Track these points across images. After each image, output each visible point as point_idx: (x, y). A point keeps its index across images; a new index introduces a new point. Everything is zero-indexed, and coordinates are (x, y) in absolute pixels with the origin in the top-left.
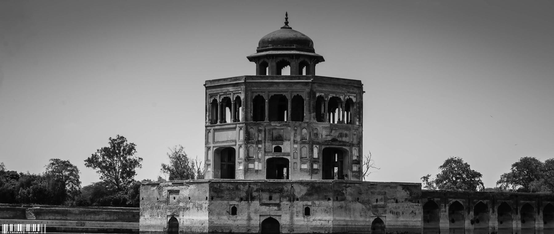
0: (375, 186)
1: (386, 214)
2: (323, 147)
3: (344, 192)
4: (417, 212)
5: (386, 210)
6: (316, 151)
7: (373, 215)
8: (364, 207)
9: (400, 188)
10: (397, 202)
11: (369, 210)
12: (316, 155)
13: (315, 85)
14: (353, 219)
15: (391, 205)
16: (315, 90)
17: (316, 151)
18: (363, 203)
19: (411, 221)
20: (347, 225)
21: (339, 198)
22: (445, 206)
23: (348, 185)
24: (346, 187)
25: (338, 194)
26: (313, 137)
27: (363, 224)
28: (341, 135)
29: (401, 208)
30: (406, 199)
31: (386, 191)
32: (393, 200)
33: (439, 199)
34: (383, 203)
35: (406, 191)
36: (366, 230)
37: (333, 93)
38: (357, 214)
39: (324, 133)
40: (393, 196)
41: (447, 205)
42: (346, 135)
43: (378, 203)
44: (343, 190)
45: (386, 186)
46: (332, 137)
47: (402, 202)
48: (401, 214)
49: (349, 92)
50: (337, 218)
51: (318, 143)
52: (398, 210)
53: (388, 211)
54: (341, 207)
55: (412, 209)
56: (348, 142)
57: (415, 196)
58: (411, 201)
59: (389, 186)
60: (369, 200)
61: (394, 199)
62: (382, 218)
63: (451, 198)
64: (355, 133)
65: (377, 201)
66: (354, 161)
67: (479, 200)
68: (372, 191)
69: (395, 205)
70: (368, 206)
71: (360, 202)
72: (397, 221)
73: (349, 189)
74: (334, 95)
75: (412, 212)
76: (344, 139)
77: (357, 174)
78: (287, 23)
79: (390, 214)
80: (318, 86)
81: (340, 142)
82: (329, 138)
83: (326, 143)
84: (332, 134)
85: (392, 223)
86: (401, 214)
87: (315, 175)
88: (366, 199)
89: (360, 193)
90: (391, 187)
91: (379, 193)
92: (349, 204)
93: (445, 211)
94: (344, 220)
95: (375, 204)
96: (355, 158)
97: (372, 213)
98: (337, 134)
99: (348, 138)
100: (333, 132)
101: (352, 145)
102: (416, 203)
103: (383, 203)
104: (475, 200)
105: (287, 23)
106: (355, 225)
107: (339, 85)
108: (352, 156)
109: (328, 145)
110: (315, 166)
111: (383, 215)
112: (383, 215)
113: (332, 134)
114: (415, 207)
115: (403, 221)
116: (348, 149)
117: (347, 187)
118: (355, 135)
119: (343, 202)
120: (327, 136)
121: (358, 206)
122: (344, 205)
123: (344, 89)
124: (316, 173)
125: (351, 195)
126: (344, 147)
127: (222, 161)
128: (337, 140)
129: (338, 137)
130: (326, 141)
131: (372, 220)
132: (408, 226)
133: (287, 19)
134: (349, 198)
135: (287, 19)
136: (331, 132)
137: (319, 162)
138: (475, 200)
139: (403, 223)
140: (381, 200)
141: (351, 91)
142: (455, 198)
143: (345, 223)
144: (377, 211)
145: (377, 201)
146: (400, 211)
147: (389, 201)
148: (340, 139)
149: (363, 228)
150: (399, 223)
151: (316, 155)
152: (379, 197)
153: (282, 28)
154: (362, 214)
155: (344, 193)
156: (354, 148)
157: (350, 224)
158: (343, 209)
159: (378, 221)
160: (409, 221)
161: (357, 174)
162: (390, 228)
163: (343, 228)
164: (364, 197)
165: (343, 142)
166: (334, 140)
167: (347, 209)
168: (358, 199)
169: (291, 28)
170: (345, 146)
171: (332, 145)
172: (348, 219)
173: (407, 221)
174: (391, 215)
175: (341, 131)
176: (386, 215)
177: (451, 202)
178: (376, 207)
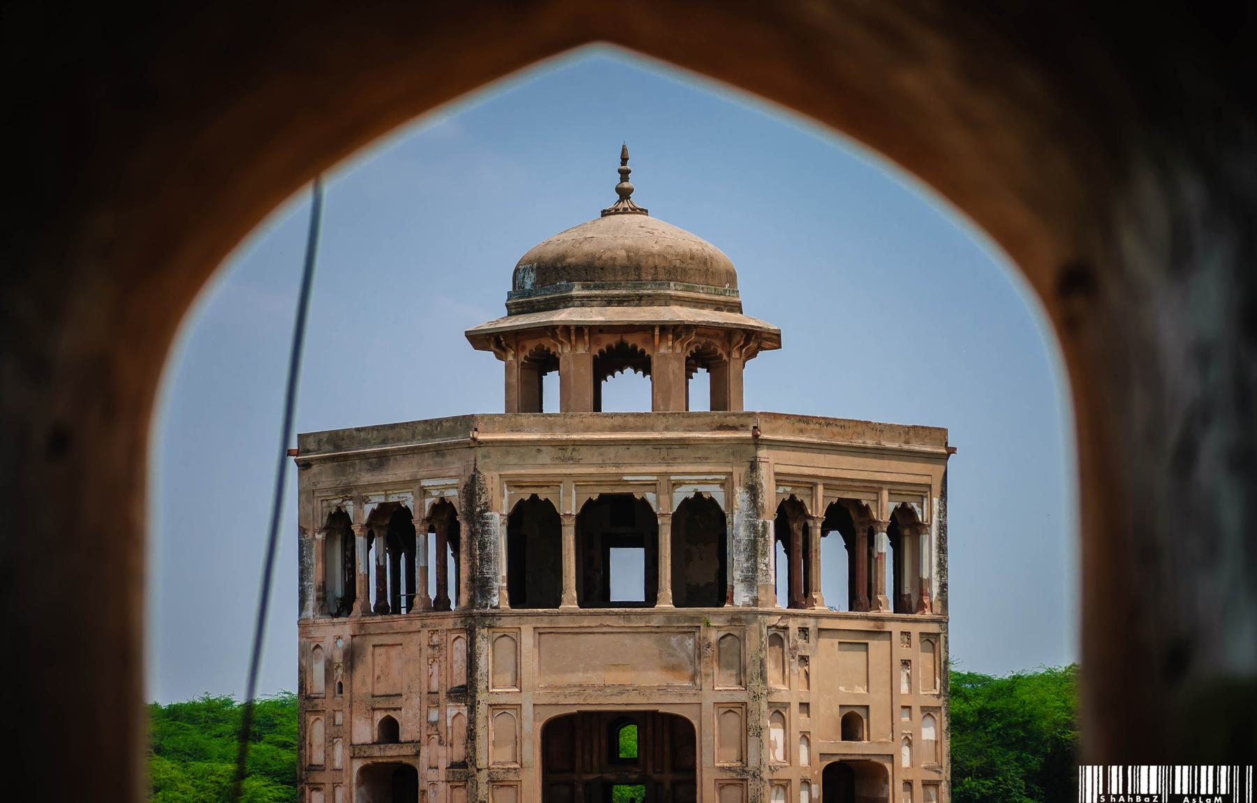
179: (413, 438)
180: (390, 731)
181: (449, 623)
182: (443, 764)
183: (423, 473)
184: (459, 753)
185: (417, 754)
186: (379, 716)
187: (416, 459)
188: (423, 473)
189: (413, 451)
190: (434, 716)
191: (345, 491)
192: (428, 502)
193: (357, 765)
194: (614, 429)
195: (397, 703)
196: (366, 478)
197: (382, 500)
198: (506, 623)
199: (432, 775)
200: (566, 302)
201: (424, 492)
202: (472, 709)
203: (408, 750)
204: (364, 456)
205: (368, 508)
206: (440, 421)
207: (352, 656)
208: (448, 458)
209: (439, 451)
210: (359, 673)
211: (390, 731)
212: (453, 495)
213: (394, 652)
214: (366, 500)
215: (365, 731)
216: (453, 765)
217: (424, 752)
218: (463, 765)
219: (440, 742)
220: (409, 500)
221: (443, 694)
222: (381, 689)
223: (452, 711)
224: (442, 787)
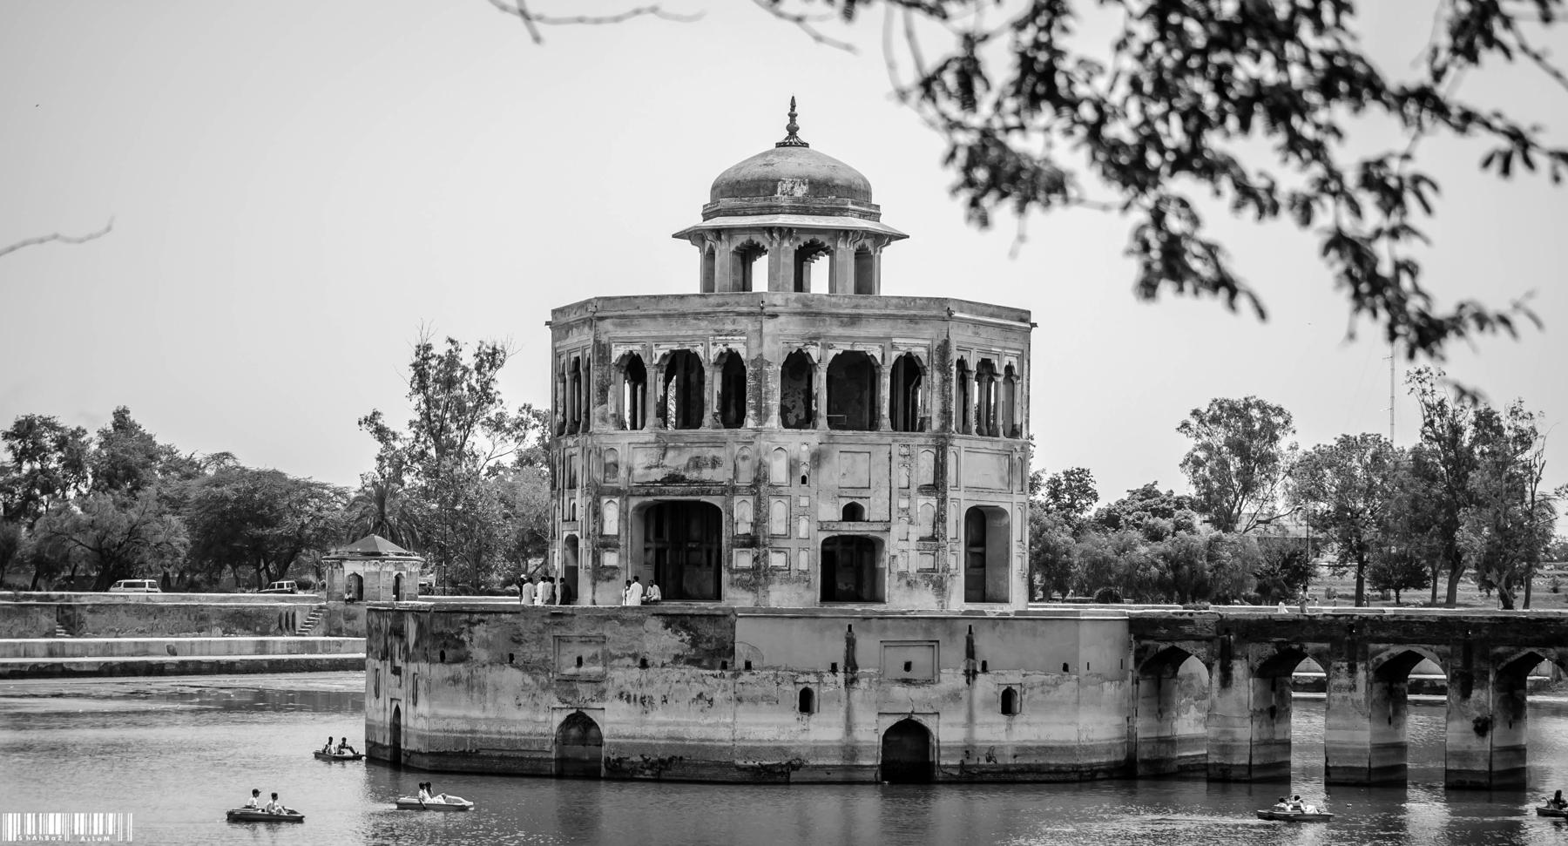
0: (566, 619)
1: (605, 700)
2: (634, 502)
3: (464, 637)
4: (718, 696)
5: (604, 691)
6: (611, 515)
7: (558, 704)
8: (528, 680)
9: (654, 624)
10: (644, 664)
11: (545, 688)
12: (611, 526)
13: (607, 325)
14: (492, 715)
15: (624, 675)
16: (604, 339)
17: (611, 515)
18: (527, 668)
19: (696, 724)
20: (472, 731)
21: (449, 654)
22: (1352, 670)
23: (476, 617)
24: (471, 624)
25: (445, 644)
26: (599, 476)
27: (526, 729)
28: (697, 463)
29: (658, 685)
30: (677, 658)
31: (607, 633)
32: (629, 661)
33: (1326, 646)
34: (598, 669)
35: (676, 632)
36: (535, 747)
37: (669, 340)
38: (507, 702)
39: (640, 460)
40: (632, 647)
41: (1360, 666)
42: (715, 463)
43: (583, 669)
44: (460, 631)
45: (608, 618)
46: (666, 471)
47: (663, 665)
48: (658, 701)
49: (719, 333)
50: (443, 712)
51: (617, 492)
52: (647, 691)
53: (611, 694)
54: (455, 680)
55: (699, 687)
56: (717, 484)
57: (712, 646)
58: (691, 662)
59: (616, 618)
60: (545, 661)
61: (635, 656)
62: (589, 713)
63: (1379, 640)
64: (746, 453)
65: (580, 662)
66: (739, 536)
67: (1520, 646)
68: (557, 633)
69: (636, 673)
70: (543, 679)
71: (517, 667)
72: (643, 724)
73: (479, 630)
74: (676, 347)
75: (700, 696)
76: (707, 474)
77: (746, 577)
78: (792, 130)
79: (617, 701)
80: (615, 325)
81: (691, 482)
82: (657, 474)
83: (642, 491)
84: (666, 462)
85: (627, 730)
86: (658, 701)
87: (605, 584)
88: (538, 656)
89: (518, 641)
90: (623, 622)
91: (586, 640)
92: (481, 672)
93: (1353, 688)
94: (464, 717)
95: (572, 670)
96: (744, 529)
97: (555, 699)
98: (683, 460)
99: (719, 470)
100: (671, 454)
101: (731, 490)
102: (712, 667)
103: (598, 669)
104: (1500, 649)
105: (792, 130)
106: (499, 732)
107: (684, 315)
108: (734, 523)
109: (648, 494)
110: (610, 559)
111: (595, 705)
112: (595, 705)
113: (666, 462)
114: (709, 680)
115: (665, 724)
116: (719, 505)
117: (474, 624)
118: (744, 458)
119: (460, 666)
120: (650, 468)
121: (512, 677)
122: (465, 675)
123: (703, 324)
124: (609, 579)
125: (487, 644)
126: (704, 499)
127: (647, 540)
128: (683, 479)
129: (687, 468)
130: (643, 485)
131: (559, 718)
132: (683, 739)
133: (793, 116)
134: (481, 654)
135: (793, 116)
136: (664, 455)
137: (618, 546)
138: (1500, 649)
139: (666, 729)
140: (594, 659)
141: (729, 327)
142: (1398, 641)
143: (466, 727)
144: (574, 693)
145: (580, 662)
146: (655, 692)
147: (616, 662)
148: (692, 475)
149: (525, 742)
150: (651, 730)
151: (611, 526)
152: (587, 652)
153: (779, 145)
154: (522, 701)
155: (462, 642)
156: (737, 499)
157: (484, 728)
158: (461, 687)
159: (580, 723)
160: (687, 724)
161: (746, 577)
162: (617, 745)
163: (458, 741)
164: (530, 652)
165: (703, 482)
166: (673, 479)
167: (473, 686)
168: (512, 657)
169: (807, 145)
170: (708, 493)
171: (662, 493)
172: (476, 713)
173: (679, 724)
174: (624, 704)
175: (695, 452)
176: (605, 705)
177: (1384, 657)
178: (571, 680)
179: (886, 307)
180: (852, 512)
181: (922, 440)
182: (914, 538)
183: (895, 333)
184: (927, 530)
185: (888, 530)
186: (845, 502)
187: (889, 323)
188: (895, 333)
189: (887, 317)
190: (904, 503)
191: (813, 339)
192: (895, 355)
193: (823, 536)
194: (992, 316)
195: (865, 493)
196: (837, 331)
197: (848, 348)
198: (956, 442)
199: (904, 545)
200: (841, 211)
201: (893, 347)
202: (943, 501)
203: (879, 527)
204: (837, 316)
205: (832, 354)
206: (914, 299)
207: (817, 458)
208: (921, 325)
209: (912, 319)
210: (825, 471)
211: (852, 512)
212: (920, 352)
213: (859, 457)
214: (831, 347)
215: (831, 512)
216: (921, 539)
217: (897, 530)
218: (933, 538)
219: (910, 522)
220: (876, 352)
221: (914, 489)
222: (847, 482)
223: (921, 500)
224: (914, 554)
